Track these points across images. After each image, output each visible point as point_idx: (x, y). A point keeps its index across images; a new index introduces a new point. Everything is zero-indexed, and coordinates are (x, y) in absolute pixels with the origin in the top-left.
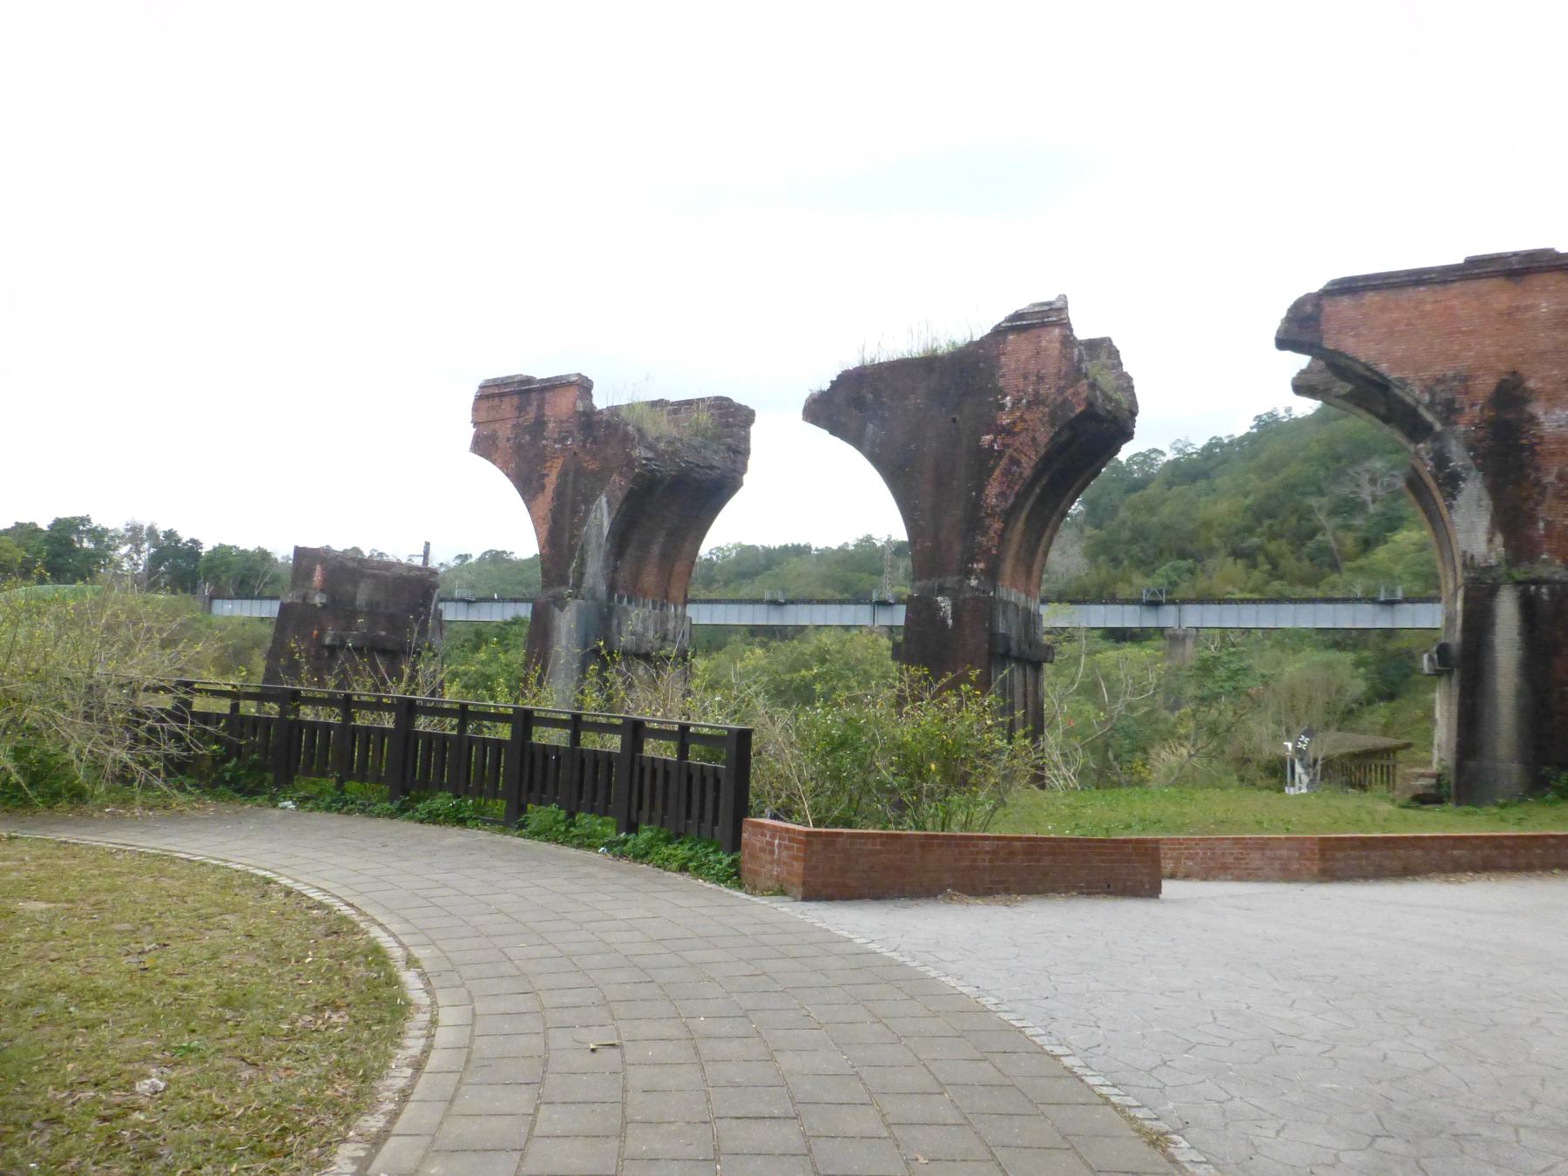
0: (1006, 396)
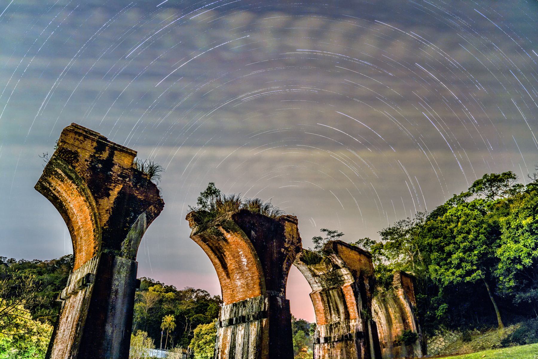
0: (286, 239)
